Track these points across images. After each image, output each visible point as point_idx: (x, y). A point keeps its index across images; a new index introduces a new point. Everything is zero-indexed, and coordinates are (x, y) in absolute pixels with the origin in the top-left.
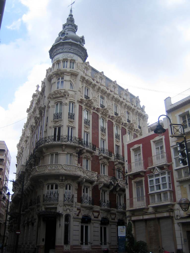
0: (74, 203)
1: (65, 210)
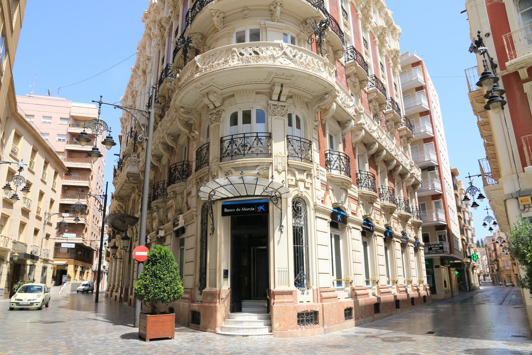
0: (315, 166)
1: (293, 183)
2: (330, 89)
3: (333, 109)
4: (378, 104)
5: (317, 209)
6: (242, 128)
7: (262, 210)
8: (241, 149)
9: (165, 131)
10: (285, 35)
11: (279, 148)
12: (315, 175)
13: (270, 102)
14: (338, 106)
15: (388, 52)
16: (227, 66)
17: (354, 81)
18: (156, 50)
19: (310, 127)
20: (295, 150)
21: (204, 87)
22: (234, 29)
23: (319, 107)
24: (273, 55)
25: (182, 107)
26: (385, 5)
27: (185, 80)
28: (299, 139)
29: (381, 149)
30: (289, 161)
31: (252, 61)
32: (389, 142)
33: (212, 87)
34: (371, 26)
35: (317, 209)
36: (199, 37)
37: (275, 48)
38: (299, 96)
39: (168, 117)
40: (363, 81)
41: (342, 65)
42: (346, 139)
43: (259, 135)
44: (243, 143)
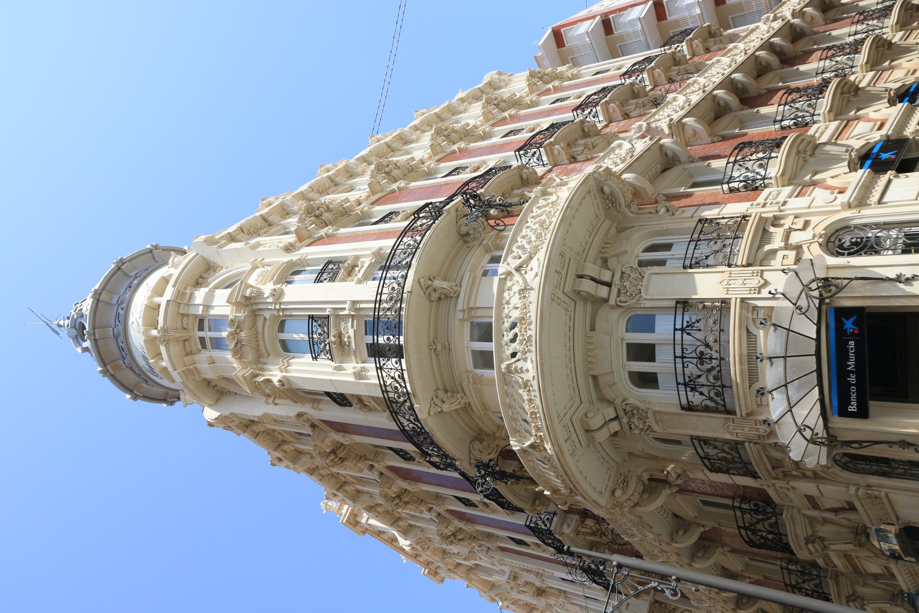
1: (792, 254)
2: (592, 182)
3: (635, 178)
4: (632, 100)
5: (861, 202)
6: (663, 364)
7: (853, 324)
8: (709, 366)
9: (665, 547)
10: (485, 273)
11: (708, 285)
12: (776, 208)
13: (612, 302)
14: (627, 170)
15: (531, 92)
16: (535, 383)
17: (581, 148)
18: (498, 555)
19: (668, 223)
20: (717, 252)
21: (574, 437)
22: (467, 371)
23: (628, 206)
24: (520, 291)
25: (613, 492)
26: (446, 104)
27: (557, 477)
28: (693, 244)
29: (728, 84)
30: (739, 263)
31: (529, 333)
32: (713, 71)
33: (573, 419)
34: (482, 125)
35: (861, 202)
36: (477, 445)
37: (506, 288)
38: (605, 244)
39: (633, 536)
40: (583, 130)
41: (550, 171)
42: (702, 155)
43: (679, 326)
44: (695, 361)
